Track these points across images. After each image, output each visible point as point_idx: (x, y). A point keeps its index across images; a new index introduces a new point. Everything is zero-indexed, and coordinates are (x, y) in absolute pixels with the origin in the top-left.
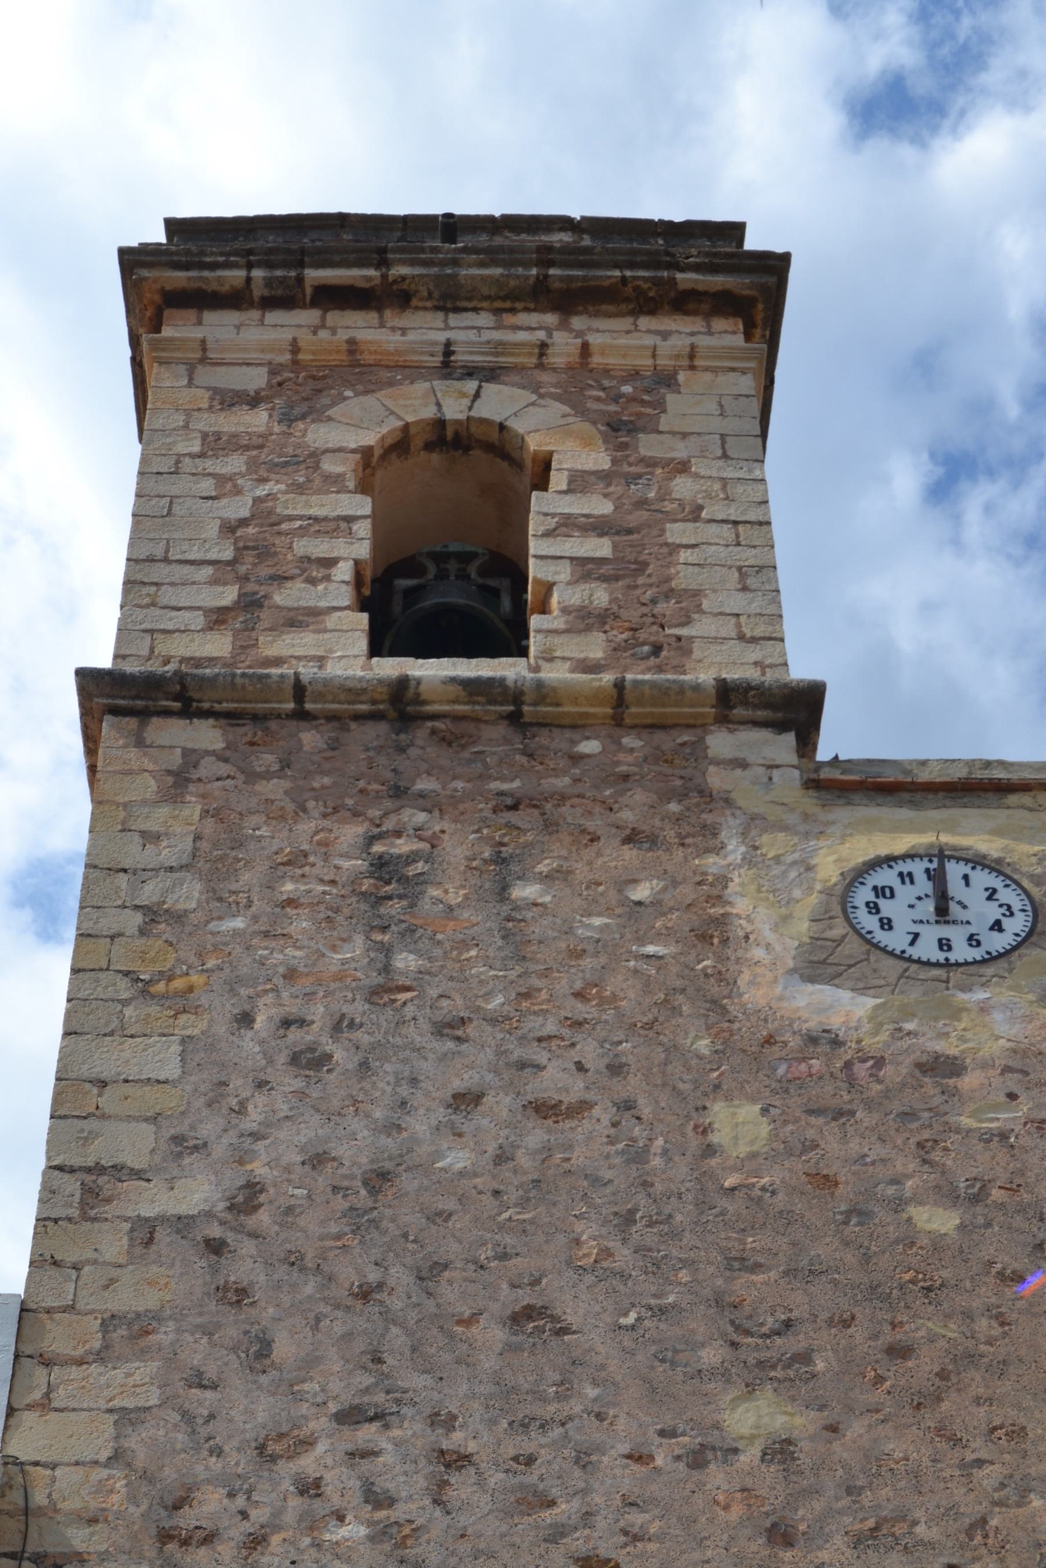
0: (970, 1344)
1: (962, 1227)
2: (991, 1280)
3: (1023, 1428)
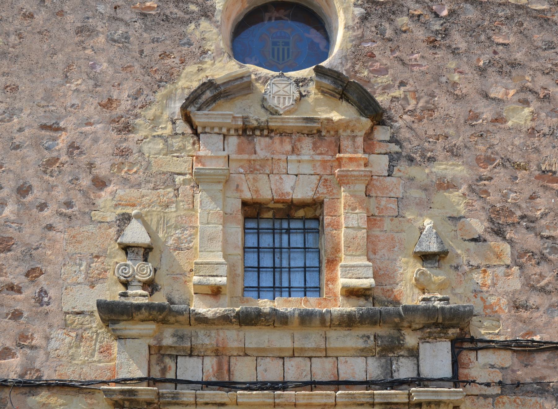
0: (6, 47)
2: (20, 17)
3: (18, 87)
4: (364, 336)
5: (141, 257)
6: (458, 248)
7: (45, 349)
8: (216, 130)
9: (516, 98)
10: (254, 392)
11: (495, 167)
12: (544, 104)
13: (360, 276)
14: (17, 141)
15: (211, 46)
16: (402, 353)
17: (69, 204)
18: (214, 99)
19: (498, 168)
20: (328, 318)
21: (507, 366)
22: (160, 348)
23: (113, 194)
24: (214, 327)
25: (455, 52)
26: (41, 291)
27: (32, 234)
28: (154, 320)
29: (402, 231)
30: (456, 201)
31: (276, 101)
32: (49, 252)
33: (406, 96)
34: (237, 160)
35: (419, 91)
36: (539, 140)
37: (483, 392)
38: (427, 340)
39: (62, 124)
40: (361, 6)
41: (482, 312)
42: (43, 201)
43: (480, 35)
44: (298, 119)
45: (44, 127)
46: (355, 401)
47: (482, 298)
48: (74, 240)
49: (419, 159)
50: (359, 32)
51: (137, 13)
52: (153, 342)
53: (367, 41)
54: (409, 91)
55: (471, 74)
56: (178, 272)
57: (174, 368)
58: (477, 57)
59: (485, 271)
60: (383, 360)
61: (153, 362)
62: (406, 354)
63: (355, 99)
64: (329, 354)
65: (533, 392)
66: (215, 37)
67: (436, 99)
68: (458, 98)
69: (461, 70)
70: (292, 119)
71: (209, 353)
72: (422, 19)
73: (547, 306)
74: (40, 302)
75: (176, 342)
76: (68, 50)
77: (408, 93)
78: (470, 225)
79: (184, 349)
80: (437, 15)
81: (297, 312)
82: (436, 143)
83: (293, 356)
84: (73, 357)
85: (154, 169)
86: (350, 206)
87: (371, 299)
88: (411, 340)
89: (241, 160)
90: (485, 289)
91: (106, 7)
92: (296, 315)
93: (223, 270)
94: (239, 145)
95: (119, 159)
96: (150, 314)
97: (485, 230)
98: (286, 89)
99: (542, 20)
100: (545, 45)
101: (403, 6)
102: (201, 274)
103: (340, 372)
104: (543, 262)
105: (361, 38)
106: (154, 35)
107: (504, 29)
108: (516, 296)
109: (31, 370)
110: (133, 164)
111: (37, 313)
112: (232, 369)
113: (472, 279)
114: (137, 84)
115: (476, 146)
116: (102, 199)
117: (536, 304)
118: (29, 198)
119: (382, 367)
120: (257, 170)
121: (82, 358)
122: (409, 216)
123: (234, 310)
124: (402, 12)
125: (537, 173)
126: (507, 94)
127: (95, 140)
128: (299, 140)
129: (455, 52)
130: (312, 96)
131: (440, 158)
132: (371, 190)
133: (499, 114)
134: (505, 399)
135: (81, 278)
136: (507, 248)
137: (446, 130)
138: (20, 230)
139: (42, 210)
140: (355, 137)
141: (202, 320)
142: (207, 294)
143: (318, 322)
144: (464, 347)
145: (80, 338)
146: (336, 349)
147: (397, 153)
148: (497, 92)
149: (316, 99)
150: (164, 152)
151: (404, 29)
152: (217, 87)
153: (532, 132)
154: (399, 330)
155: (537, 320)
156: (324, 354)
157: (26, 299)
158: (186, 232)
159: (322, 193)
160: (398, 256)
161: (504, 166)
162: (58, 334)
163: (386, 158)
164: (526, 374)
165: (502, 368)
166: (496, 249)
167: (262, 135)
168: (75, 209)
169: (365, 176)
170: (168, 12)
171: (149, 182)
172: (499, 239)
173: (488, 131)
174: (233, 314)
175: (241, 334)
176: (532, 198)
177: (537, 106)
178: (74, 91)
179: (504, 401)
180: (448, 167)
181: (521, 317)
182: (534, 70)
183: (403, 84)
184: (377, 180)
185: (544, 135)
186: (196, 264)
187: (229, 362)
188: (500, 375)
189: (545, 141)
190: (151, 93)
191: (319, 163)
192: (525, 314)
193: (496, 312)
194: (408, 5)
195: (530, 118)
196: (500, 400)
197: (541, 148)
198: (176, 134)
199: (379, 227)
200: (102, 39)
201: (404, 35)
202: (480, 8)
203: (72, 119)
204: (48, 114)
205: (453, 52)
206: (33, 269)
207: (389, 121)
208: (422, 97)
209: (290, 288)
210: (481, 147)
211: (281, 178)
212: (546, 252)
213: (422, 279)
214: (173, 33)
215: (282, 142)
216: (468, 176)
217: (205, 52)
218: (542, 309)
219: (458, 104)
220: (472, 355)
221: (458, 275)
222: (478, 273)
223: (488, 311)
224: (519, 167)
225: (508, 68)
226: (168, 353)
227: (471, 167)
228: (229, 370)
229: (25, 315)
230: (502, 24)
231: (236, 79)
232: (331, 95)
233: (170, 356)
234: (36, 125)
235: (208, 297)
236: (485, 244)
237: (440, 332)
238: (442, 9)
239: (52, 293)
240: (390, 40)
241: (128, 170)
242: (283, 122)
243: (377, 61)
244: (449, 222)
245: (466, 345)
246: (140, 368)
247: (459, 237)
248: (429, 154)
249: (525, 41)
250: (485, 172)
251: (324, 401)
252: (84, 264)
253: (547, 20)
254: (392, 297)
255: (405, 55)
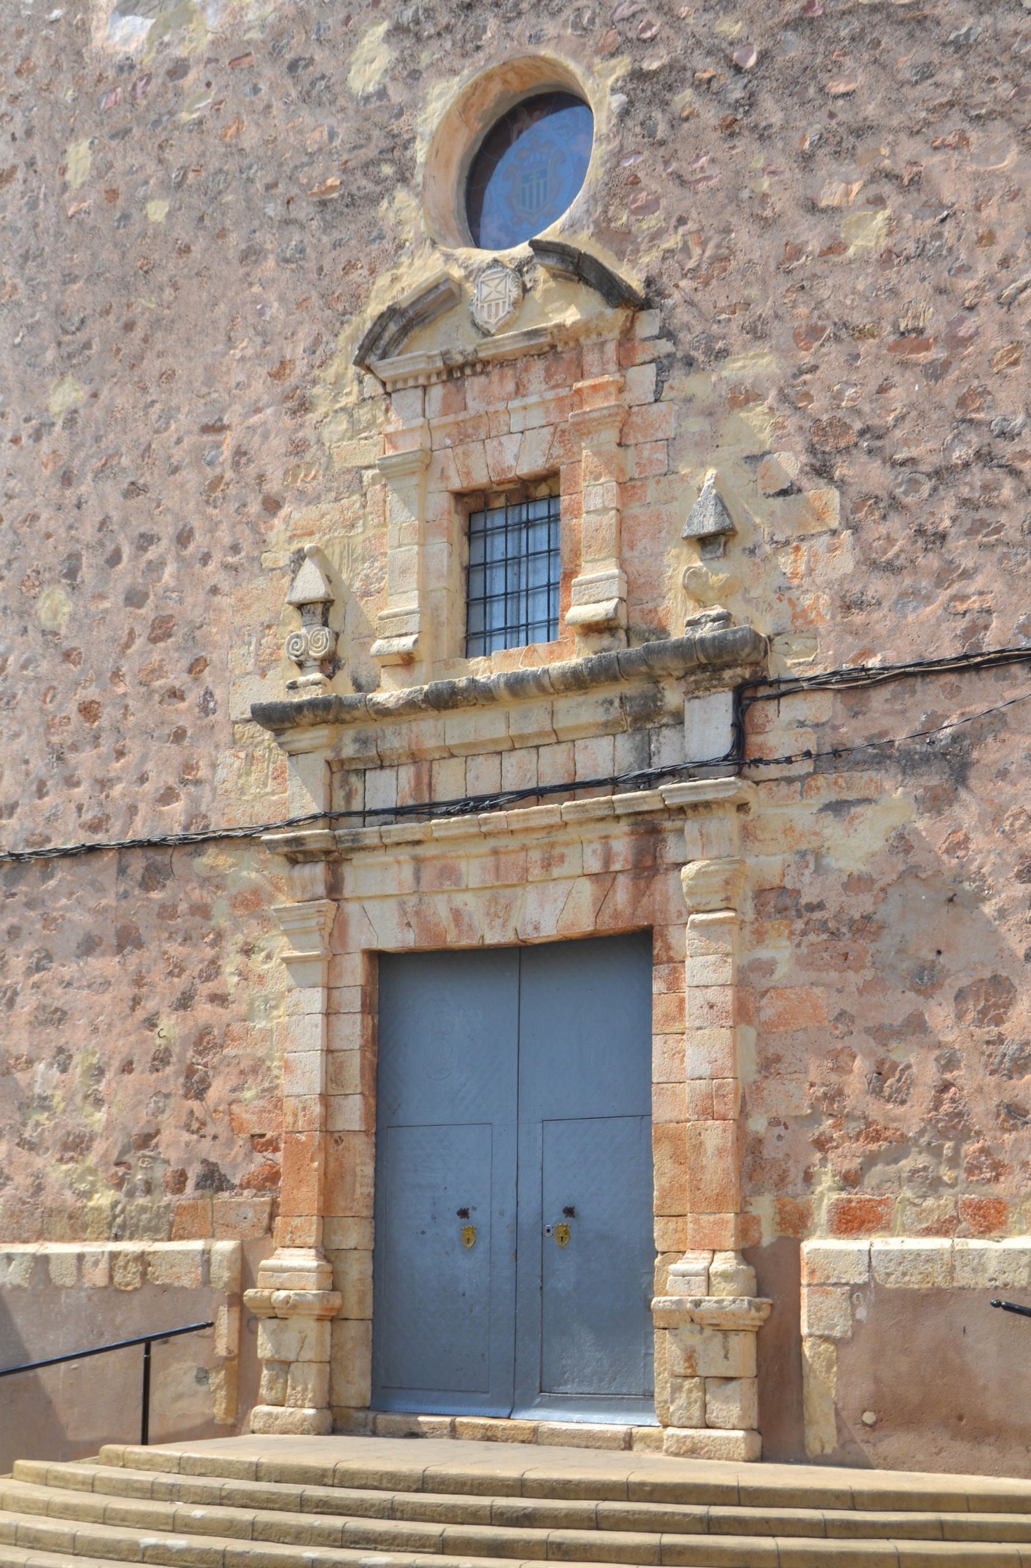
1: (169, 215)
2: (174, 255)
4: (605, 701)
5: (318, 618)
6: (756, 513)
7: (211, 782)
8: (411, 383)
9: (862, 198)
10: (453, 819)
11: (822, 345)
12: (910, 197)
13: (600, 597)
14: (174, 461)
15: (408, 234)
16: (665, 720)
17: (235, 549)
18: (404, 331)
19: (827, 344)
20: (546, 681)
21: (824, 719)
22: (342, 762)
23: (287, 520)
24: (405, 718)
25: (763, 135)
26: (206, 693)
27: (194, 606)
28: (325, 722)
29: (674, 499)
30: (759, 423)
31: (485, 314)
32: (214, 630)
33: (685, 243)
34: (440, 427)
35: (706, 229)
36: (898, 272)
37: (786, 773)
38: (697, 693)
39: (226, 421)
40: (621, 90)
41: (790, 628)
42: (206, 550)
43: (806, 88)
44: (515, 336)
45: (206, 429)
46: (587, 815)
47: (790, 600)
48: (242, 605)
49: (701, 358)
50: (615, 144)
51: (314, 204)
52: (330, 755)
53: (627, 157)
54: (690, 233)
55: (789, 171)
56: (366, 633)
57: (361, 792)
58: (800, 133)
59: (797, 549)
60: (638, 737)
61: (336, 784)
62: (671, 722)
63: (594, 281)
64: (562, 738)
65: (865, 762)
66: (414, 214)
67: (733, 235)
68: (766, 224)
69: (772, 168)
70: (508, 338)
71: (403, 759)
72: (715, 86)
73: (894, 597)
74: (205, 711)
75: (358, 751)
76: (230, 294)
77: (688, 237)
78: (778, 464)
79: (371, 760)
80: (738, 69)
81: (502, 680)
82: (729, 320)
83: (513, 749)
84: (242, 792)
85: (337, 467)
86: (591, 473)
87: (622, 634)
88: (672, 697)
89: (446, 425)
90: (796, 582)
91: (276, 204)
92: (502, 685)
93: (414, 623)
94: (445, 397)
95: (294, 460)
96: (316, 716)
97: (801, 471)
98: (499, 288)
99: (913, 24)
100: (916, 74)
101: (685, 69)
102: (387, 634)
103: (578, 765)
104: (891, 514)
105: (620, 152)
106: (336, 235)
107: (848, 62)
108: (846, 586)
109: (196, 816)
110: (310, 465)
111: (202, 728)
112: (434, 781)
113: (777, 567)
114: (315, 327)
115: (795, 311)
116: (275, 530)
117: (877, 596)
118: (191, 548)
119: (636, 749)
120: (469, 436)
121: (252, 791)
122: (684, 471)
123: (422, 689)
124: (683, 82)
125: (892, 338)
126: (847, 194)
127: (265, 436)
128: (526, 369)
129: (763, 135)
130: (541, 287)
131: (736, 348)
132: (628, 434)
133: (834, 237)
134: (821, 781)
135: (250, 668)
136: (833, 496)
137: (746, 293)
138: (181, 601)
139: (205, 564)
140: (603, 344)
141: (383, 712)
142: (398, 665)
143: (535, 691)
144: (759, 695)
145: (251, 759)
146: (569, 729)
147: (669, 356)
148: (830, 196)
149: (546, 291)
150: (349, 434)
151: (685, 114)
152: (402, 312)
153: (888, 258)
154: (657, 682)
155: (877, 627)
156: (553, 739)
157: (190, 709)
158: (376, 564)
159: (558, 457)
160: (666, 545)
161: (837, 339)
162: (225, 756)
163: (652, 369)
164: (855, 730)
165: (817, 725)
166: (817, 504)
167: (474, 374)
168: (243, 554)
169: (610, 415)
170: (353, 189)
171: (330, 490)
172: (822, 482)
173: (815, 275)
174: (421, 697)
175: (440, 723)
176: (882, 390)
177: (896, 204)
178: (239, 361)
179: (819, 784)
180: (747, 362)
181: (850, 624)
182: (895, 131)
183: (682, 221)
184: (637, 414)
185: (908, 259)
186: (381, 618)
187: (430, 771)
188: (814, 737)
189: (908, 271)
190: (331, 338)
191: (552, 405)
192: (858, 618)
193: (812, 622)
194: (694, 63)
195: (884, 231)
196: (813, 783)
197: (902, 287)
198: (364, 400)
199: (640, 499)
200: (271, 262)
201: (686, 125)
202: (808, 32)
203: (237, 408)
204: (209, 407)
205: (761, 137)
206: (197, 660)
207: (657, 299)
208: (710, 238)
209: (527, 625)
210: (802, 310)
211: (501, 444)
212: (899, 491)
213: (693, 585)
214: (359, 225)
215: (502, 378)
216: (778, 371)
217: (401, 247)
218: (886, 604)
219: (767, 236)
220: (771, 707)
221: (754, 564)
222: (787, 554)
223: (799, 622)
224: (862, 334)
225: (850, 141)
226: (354, 767)
227: (783, 353)
228: (430, 784)
229: (189, 734)
230: (845, 55)
231: (429, 291)
232: (566, 278)
233: (356, 771)
234: (196, 428)
235: (399, 669)
236: (800, 496)
237: (711, 679)
238: (747, 57)
239: (218, 694)
240: (662, 143)
241: (306, 476)
242: (497, 347)
243: (642, 190)
244: (746, 467)
245: (764, 691)
246: (315, 798)
247: (760, 492)
248: (720, 345)
249: (882, 77)
250: (806, 358)
251: (546, 821)
252: (254, 640)
253: (921, 21)
254: (656, 622)
255: (684, 164)
